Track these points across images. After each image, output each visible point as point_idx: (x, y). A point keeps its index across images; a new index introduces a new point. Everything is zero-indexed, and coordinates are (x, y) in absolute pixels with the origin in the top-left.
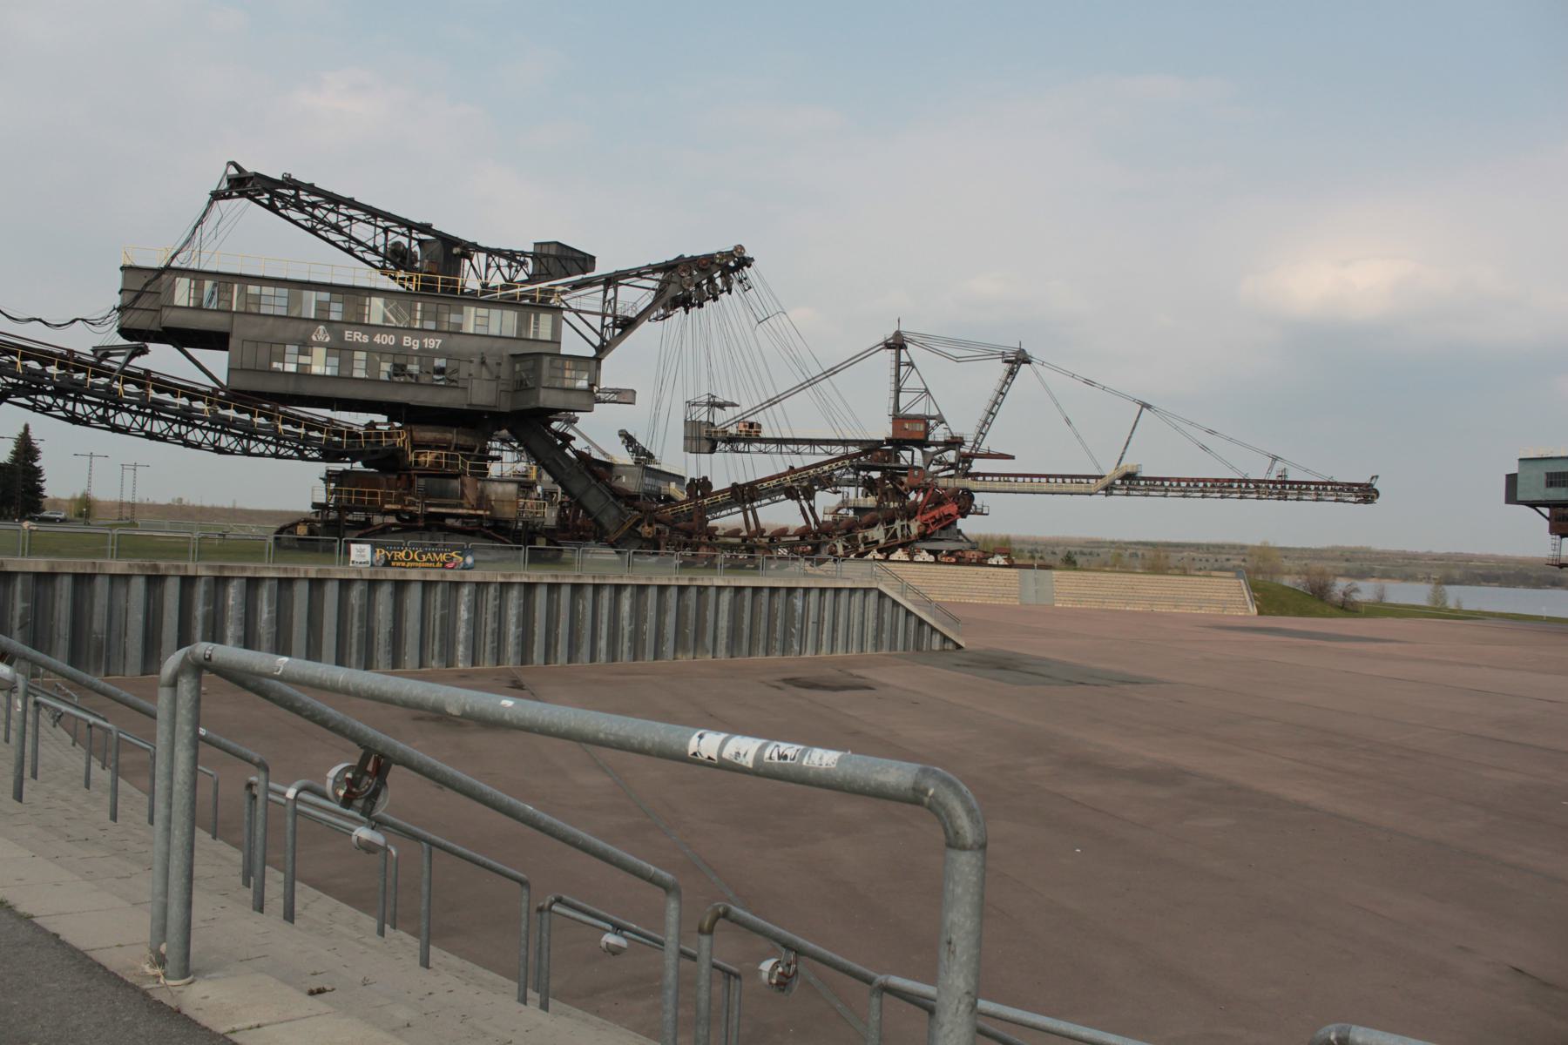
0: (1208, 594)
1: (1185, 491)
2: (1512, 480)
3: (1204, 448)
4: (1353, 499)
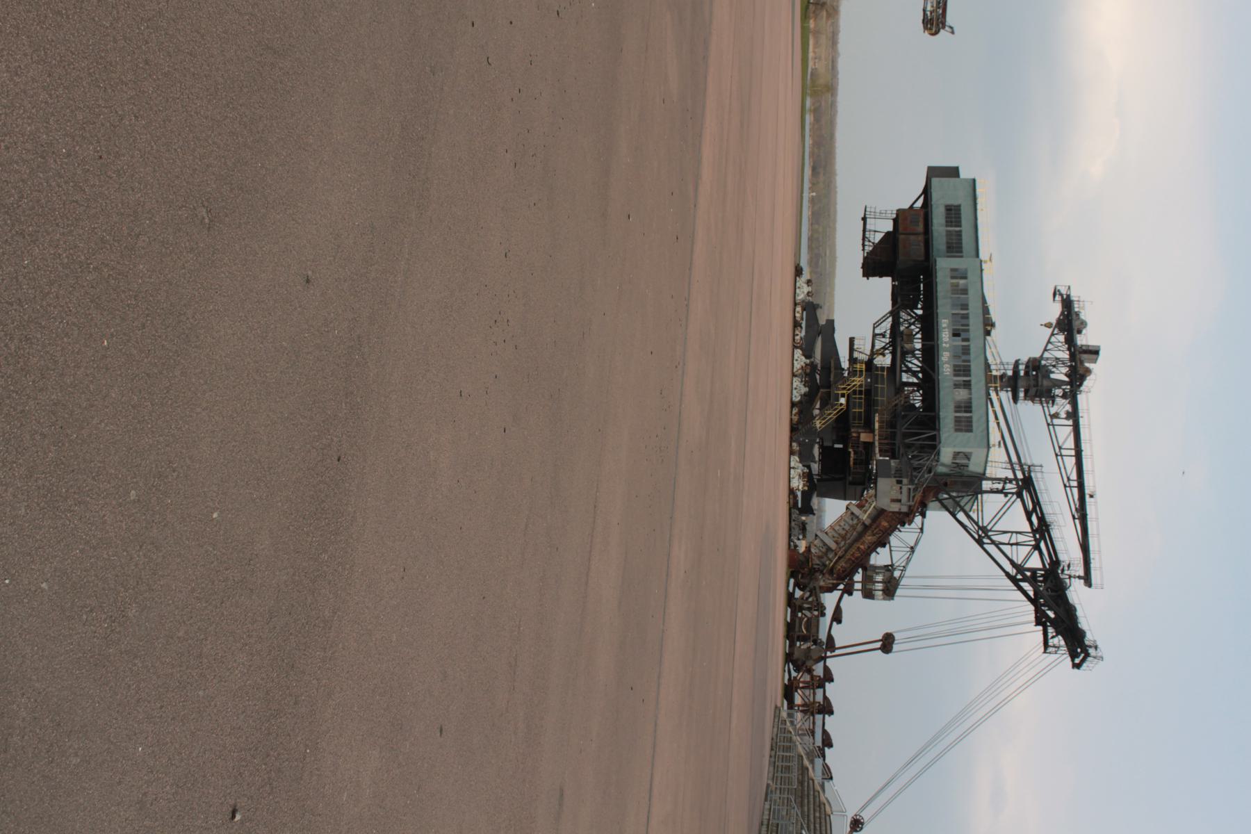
2: (953, 172)
4: (929, 8)
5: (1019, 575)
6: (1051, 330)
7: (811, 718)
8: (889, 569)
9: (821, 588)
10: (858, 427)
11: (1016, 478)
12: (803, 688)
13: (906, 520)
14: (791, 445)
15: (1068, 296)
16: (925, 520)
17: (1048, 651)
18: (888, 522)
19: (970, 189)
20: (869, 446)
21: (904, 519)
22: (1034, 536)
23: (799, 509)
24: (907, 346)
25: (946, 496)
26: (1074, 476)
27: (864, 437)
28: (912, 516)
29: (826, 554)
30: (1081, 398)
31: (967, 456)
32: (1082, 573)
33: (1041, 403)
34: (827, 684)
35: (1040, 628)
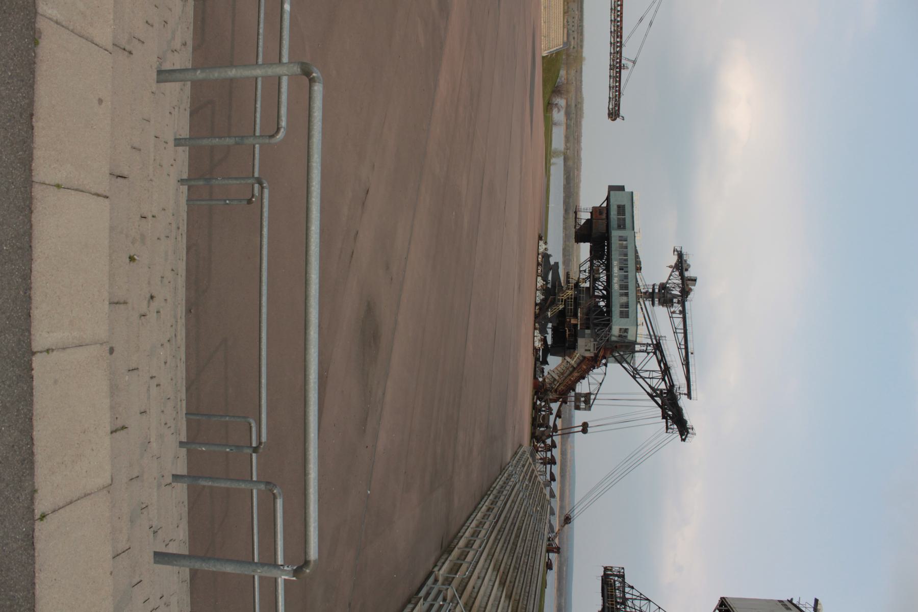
0: (553, 26)
1: (615, 10)
2: (621, 188)
3: (641, 20)
4: (611, 107)
5: (654, 394)
6: (672, 269)
7: (544, 466)
8: (587, 396)
9: (550, 399)
10: (570, 316)
11: (653, 344)
12: (541, 451)
13: (595, 365)
14: (535, 325)
15: (681, 252)
16: (607, 368)
17: (668, 431)
18: (586, 366)
19: (630, 198)
20: (576, 325)
21: (593, 362)
22: (662, 373)
23: (540, 362)
24: (597, 276)
25: (617, 354)
26: (683, 343)
27: (573, 321)
28: (598, 363)
29: (553, 382)
30: (687, 304)
31: (626, 330)
32: (686, 392)
33: (667, 307)
34: (553, 449)
35: (665, 420)
